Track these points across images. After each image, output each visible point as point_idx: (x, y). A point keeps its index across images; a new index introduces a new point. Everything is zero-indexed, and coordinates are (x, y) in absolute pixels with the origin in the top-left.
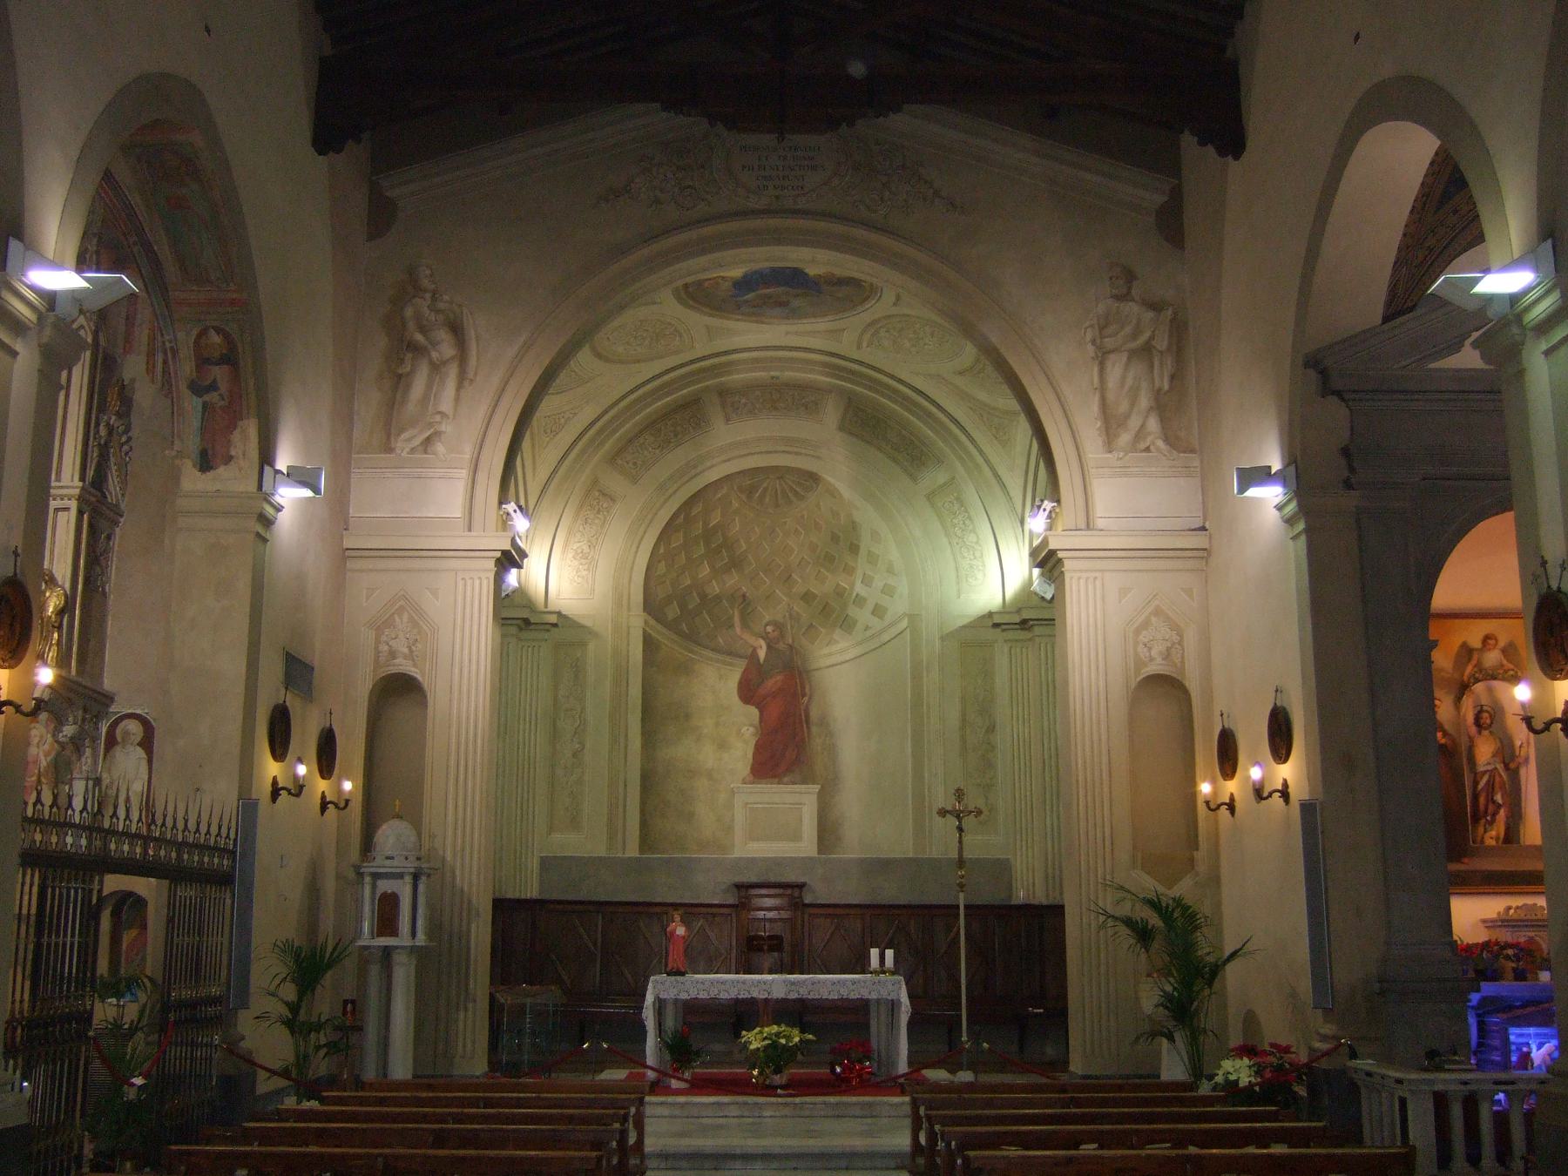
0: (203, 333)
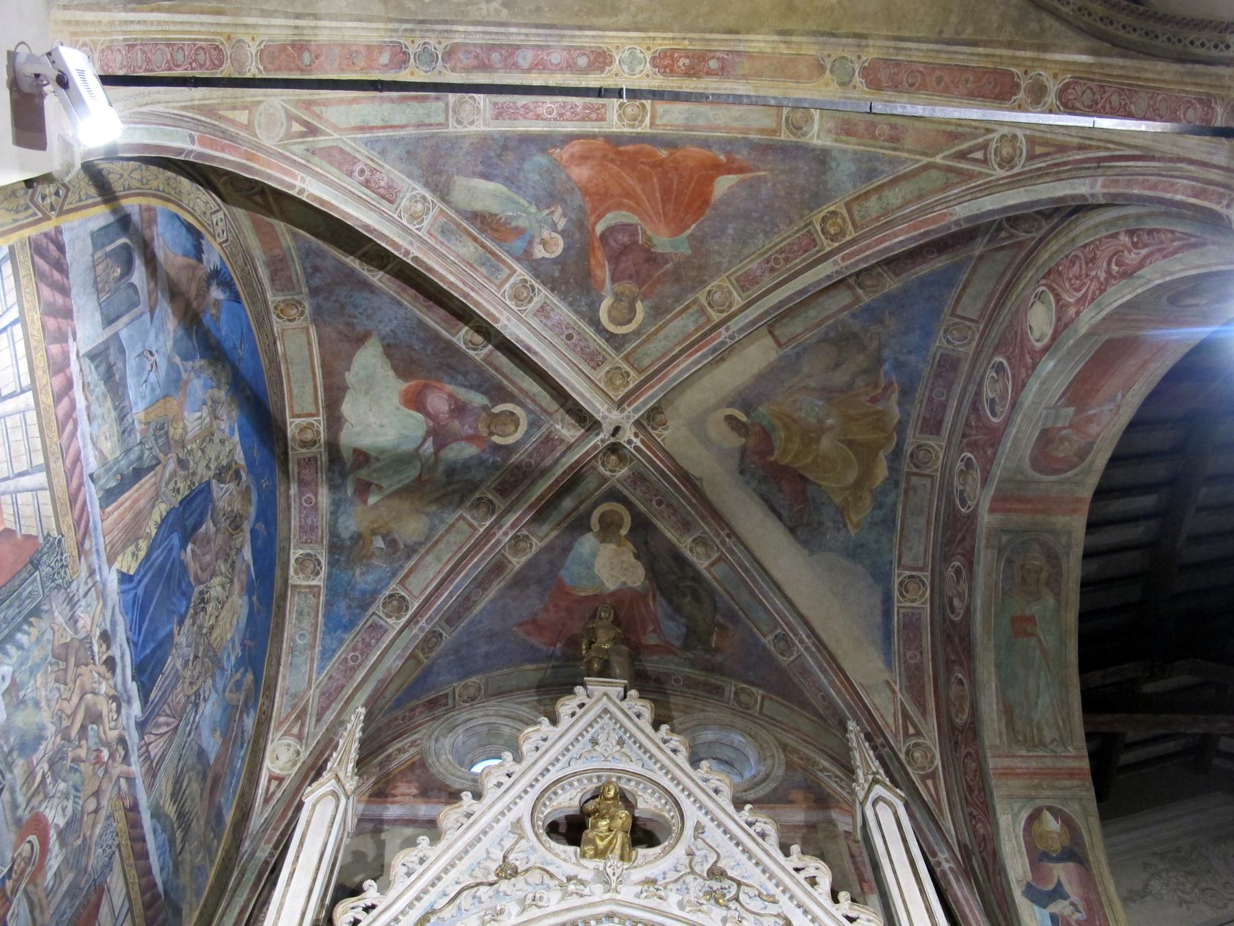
0: (1034, 817)
